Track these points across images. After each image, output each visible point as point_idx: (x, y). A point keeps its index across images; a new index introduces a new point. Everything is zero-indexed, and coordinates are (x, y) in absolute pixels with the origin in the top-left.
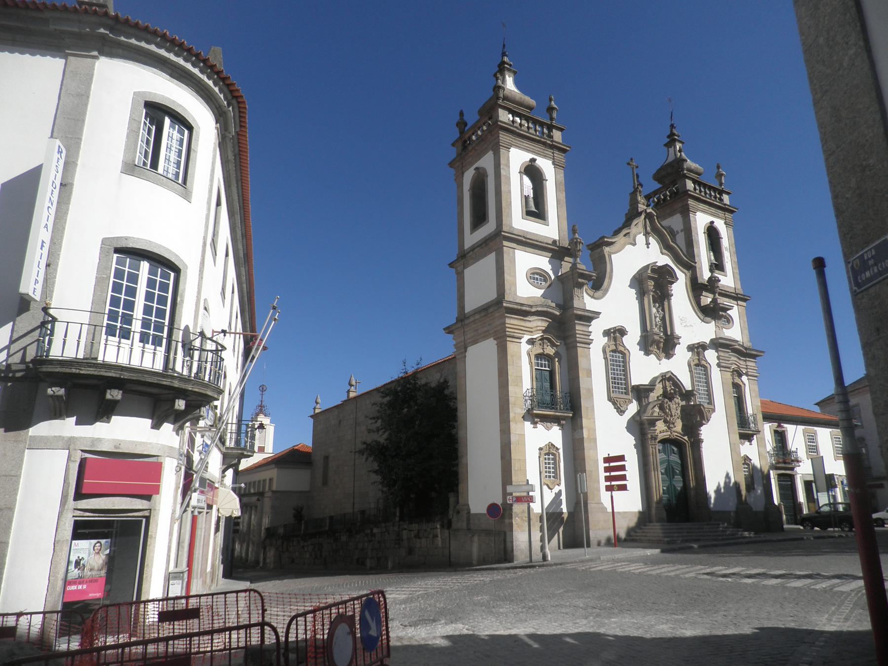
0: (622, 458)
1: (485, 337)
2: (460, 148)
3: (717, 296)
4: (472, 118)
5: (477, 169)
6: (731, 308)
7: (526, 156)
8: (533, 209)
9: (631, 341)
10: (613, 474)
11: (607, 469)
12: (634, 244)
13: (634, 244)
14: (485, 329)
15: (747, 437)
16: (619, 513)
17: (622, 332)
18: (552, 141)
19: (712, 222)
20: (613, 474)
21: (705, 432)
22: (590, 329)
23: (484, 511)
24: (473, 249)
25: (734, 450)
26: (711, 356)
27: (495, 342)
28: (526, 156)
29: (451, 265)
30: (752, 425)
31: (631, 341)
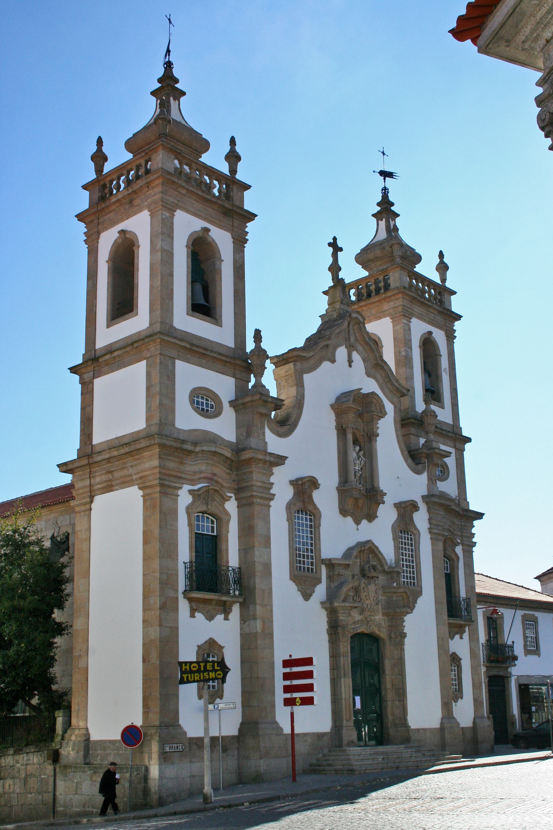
0: (308, 661)
1: (126, 483)
2: (97, 195)
3: (431, 436)
4: (118, 156)
5: (123, 232)
6: (448, 454)
7: (197, 224)
8: (202, 301)
9: (326, 499)
10: (296, 682)
11: (286, 676)
12: (333, 361)
13: (333, 361)
14: (125, 472)
15: (456, 630)
16: (298, 735)
17: (313, 483)
18: (233, 205)
19: (430, 333)
20: (296, 682)
21: (411, 623)
22: (272, 480)
23: (119, 737)
24: (110, 350)
25: (442, 647)
26: (421, 519)
27: (141, 493)
28: (197, 224)
29: (74, 370)
30: (464, 613)
31: (326, 499)
